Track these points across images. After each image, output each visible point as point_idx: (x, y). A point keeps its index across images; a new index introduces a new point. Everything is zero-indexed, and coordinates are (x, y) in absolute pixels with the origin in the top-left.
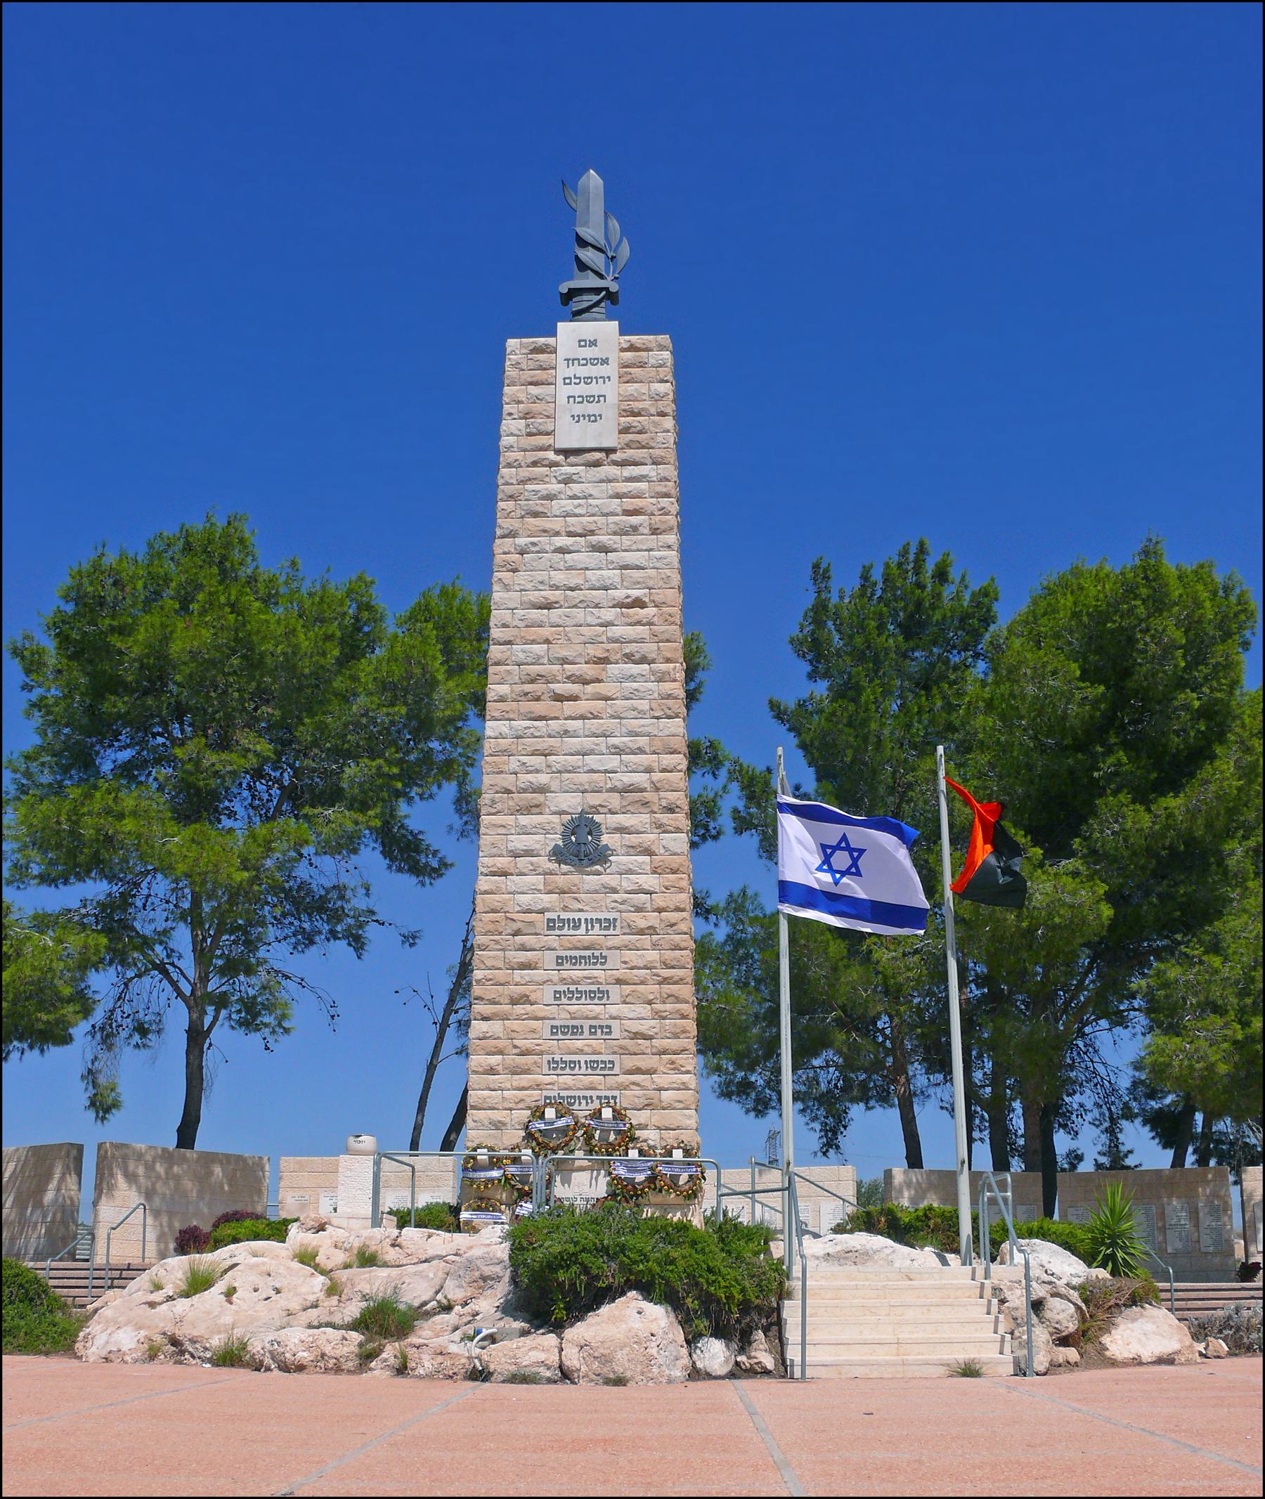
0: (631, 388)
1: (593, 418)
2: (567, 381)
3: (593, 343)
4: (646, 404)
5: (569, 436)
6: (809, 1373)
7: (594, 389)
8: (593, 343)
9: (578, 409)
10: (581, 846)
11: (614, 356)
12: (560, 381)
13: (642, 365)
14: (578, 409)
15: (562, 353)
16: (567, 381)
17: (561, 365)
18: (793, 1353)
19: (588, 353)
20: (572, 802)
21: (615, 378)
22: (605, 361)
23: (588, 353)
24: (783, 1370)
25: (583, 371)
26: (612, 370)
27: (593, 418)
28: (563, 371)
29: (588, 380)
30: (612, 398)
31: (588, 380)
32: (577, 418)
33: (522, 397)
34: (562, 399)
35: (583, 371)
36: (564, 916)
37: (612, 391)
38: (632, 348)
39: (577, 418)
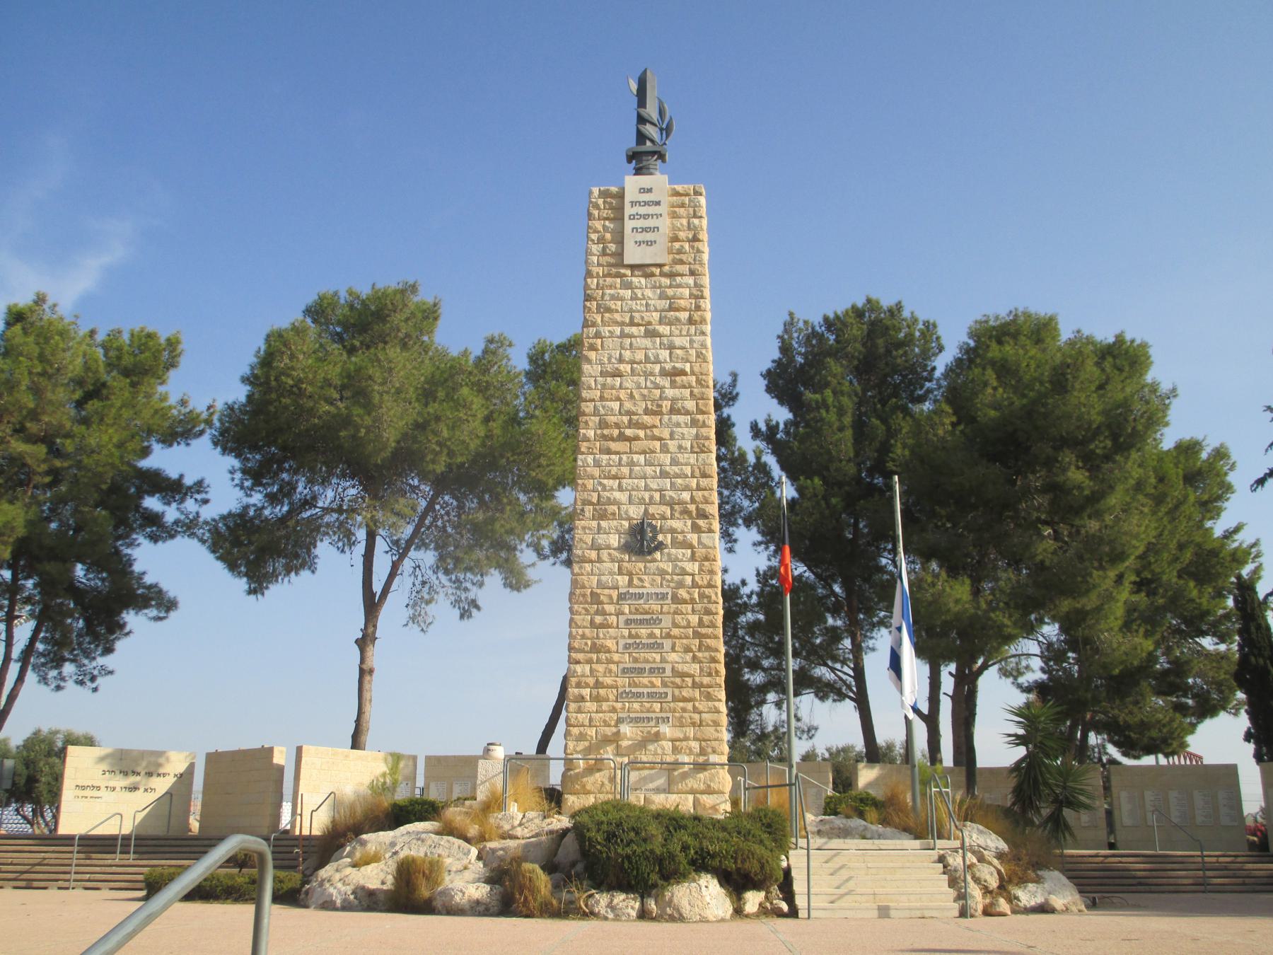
1: (650, 243)
2: (633, 203)
3: (650, 190)
5: (633, 254)
6: (813, 914)
8: (650, 190)
9: (640, 237)
10: (641, 541)
11: (666, 200)
14: (640, 237)
16: (633, 203)
18: (800, 901)
19: (646, 197)
20: (636, 512)
21: (665, 215)
22: (658, 203)
23: (646, 197)
24: (793, 913)
25: (643, 210)
26: (663, 209)
27: (650, 243)
29: (646, 217)
31: (646, 217)
32: (639, 243)
35: (643, 210)
36: (631, 590)
37: (665, 224)
38: (677, 194)
39: (639, 243)
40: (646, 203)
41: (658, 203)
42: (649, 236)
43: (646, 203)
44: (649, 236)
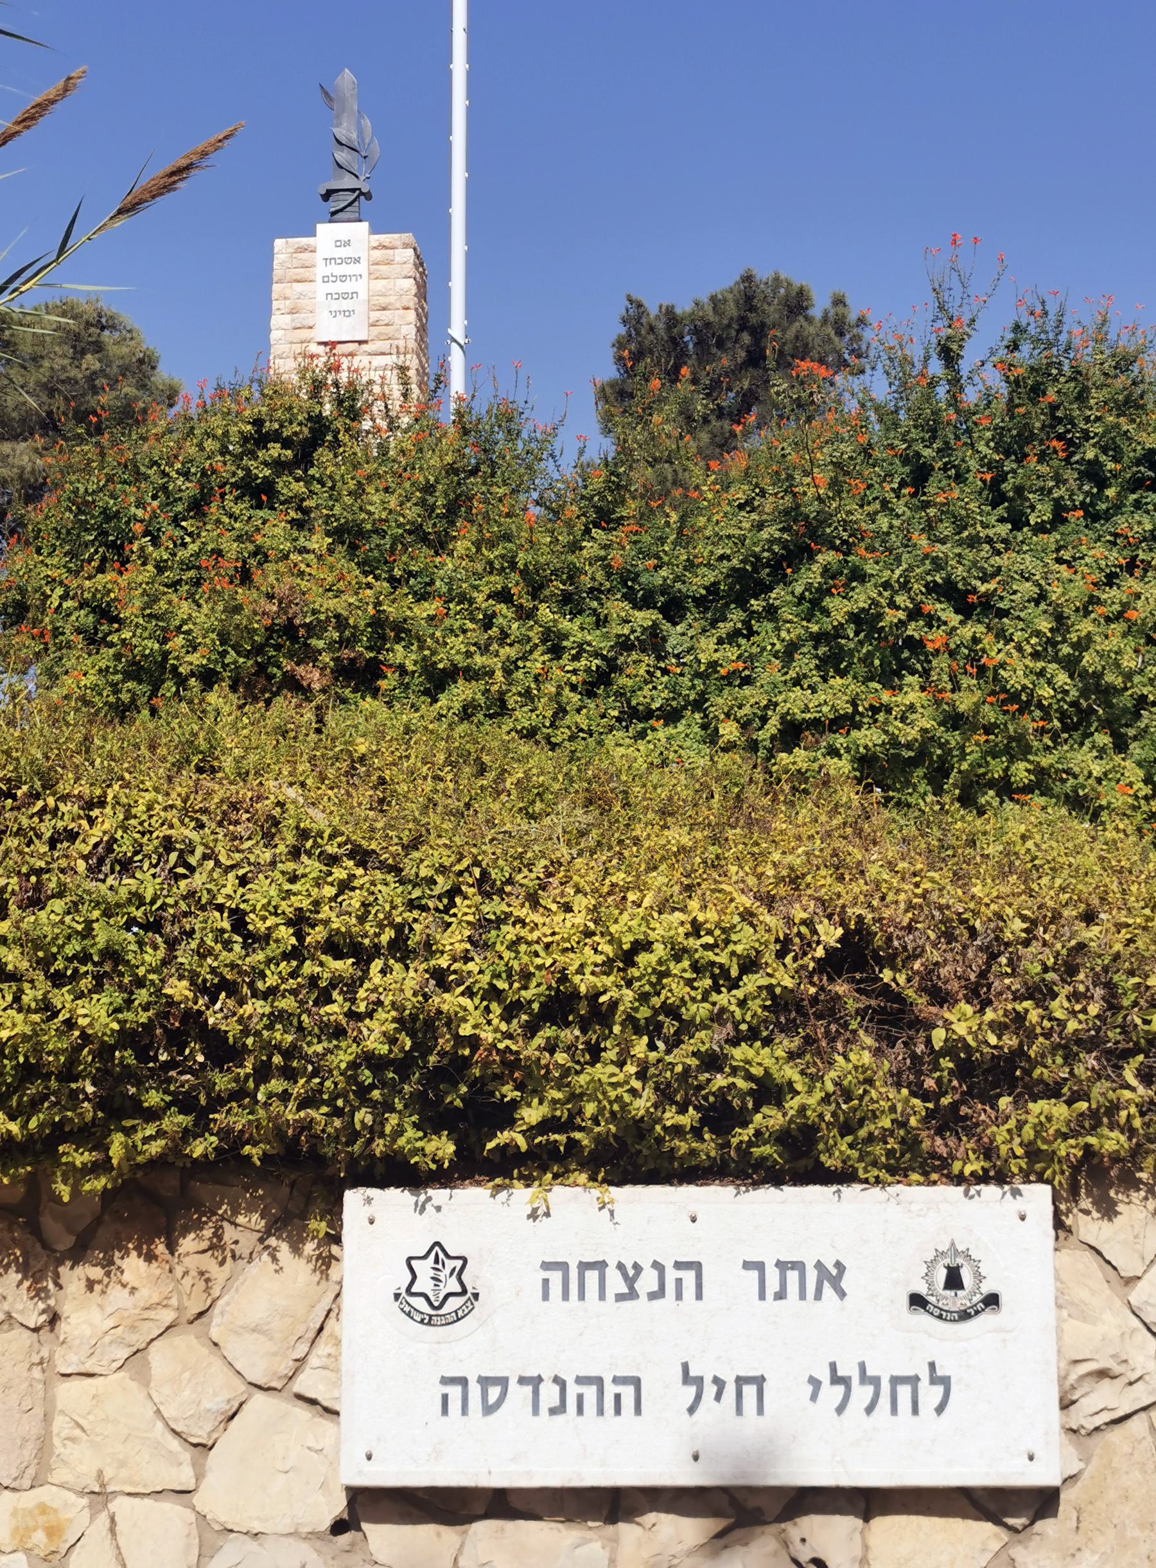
0: (380, 285)
1: (347, 313)
2: (326, 280)
3: (347, 243)
4: (392, 299)
7: (347, 287)
8: (347, 243)
9: (335, 305)
12: (319, 279)
13: (389, 263)
14: (335, 305)
15: (319, 256)
16: (326, 280)
17: (320, 264)
22: (357, 260)
26: (362, 268)
27: (347, 313)
28: (321, 270)
29: (343, 278)
30: (363, 295)
31: (343, 278)
32: (334, 314)
33: (288, 293)
34: (321, 297)
39: (334, 314)
40: (344, 261)
41: (357, 260)
42: (345, 305)
43: (344, 261)
44: (345, 305)
